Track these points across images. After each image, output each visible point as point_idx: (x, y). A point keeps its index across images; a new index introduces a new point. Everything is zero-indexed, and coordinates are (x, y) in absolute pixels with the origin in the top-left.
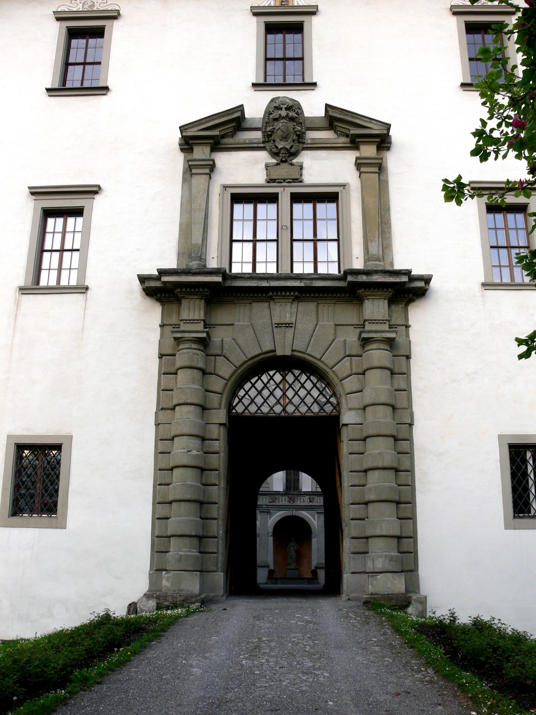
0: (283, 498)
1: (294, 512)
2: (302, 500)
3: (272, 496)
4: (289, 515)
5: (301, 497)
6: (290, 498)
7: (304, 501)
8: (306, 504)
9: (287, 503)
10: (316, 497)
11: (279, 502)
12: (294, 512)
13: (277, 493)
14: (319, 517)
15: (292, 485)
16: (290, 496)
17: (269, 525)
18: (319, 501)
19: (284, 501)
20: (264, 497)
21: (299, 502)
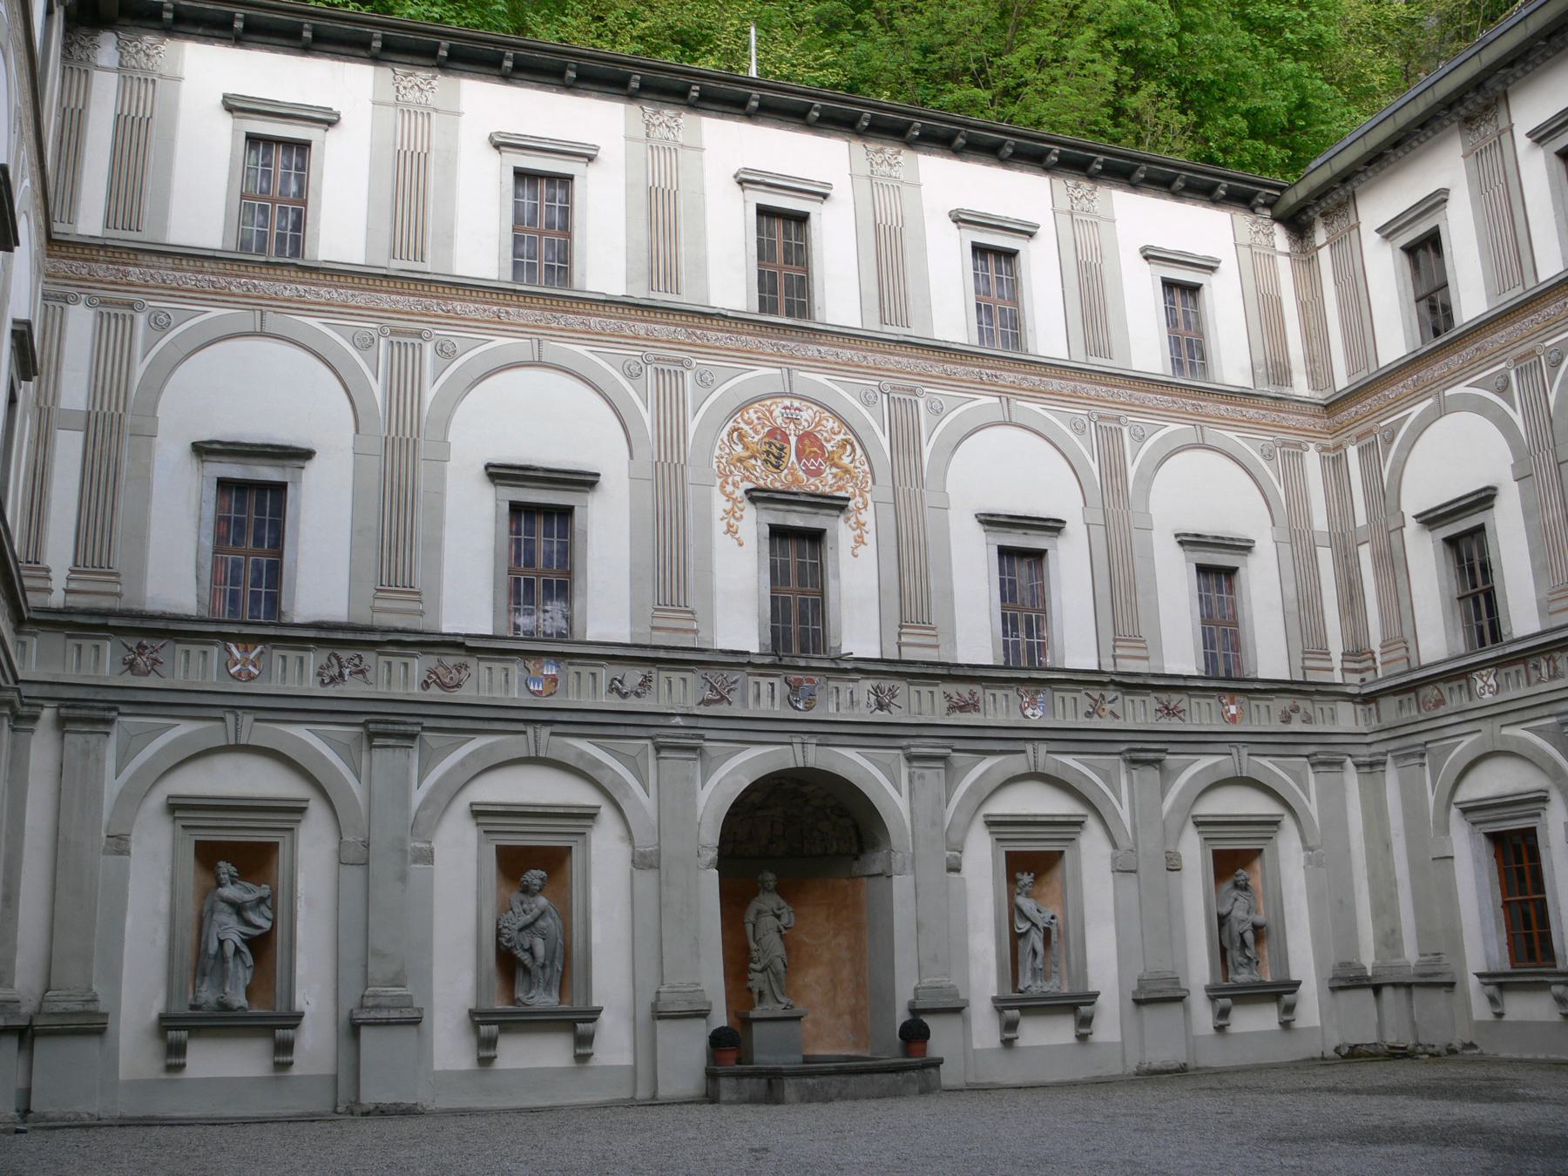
0: (765, 683)
1: (811, 749)
2: (845, 697)
3: (714, 674)
4: (792, 765)
5: (842, 686)
6: (795, 688)
7: (851, 702)
8: (864, 713)
9: (780, 710)
10: (901, 686)
11: (744, 700)
12: (811, 749)
13: (736, 661)
14: (922, 777)
15: (795, 627)
16: (793, 676)
17: (700, 811)
18: (915, 707)
19: (764, 697)
20: (676, 676)
21: (832, 708)
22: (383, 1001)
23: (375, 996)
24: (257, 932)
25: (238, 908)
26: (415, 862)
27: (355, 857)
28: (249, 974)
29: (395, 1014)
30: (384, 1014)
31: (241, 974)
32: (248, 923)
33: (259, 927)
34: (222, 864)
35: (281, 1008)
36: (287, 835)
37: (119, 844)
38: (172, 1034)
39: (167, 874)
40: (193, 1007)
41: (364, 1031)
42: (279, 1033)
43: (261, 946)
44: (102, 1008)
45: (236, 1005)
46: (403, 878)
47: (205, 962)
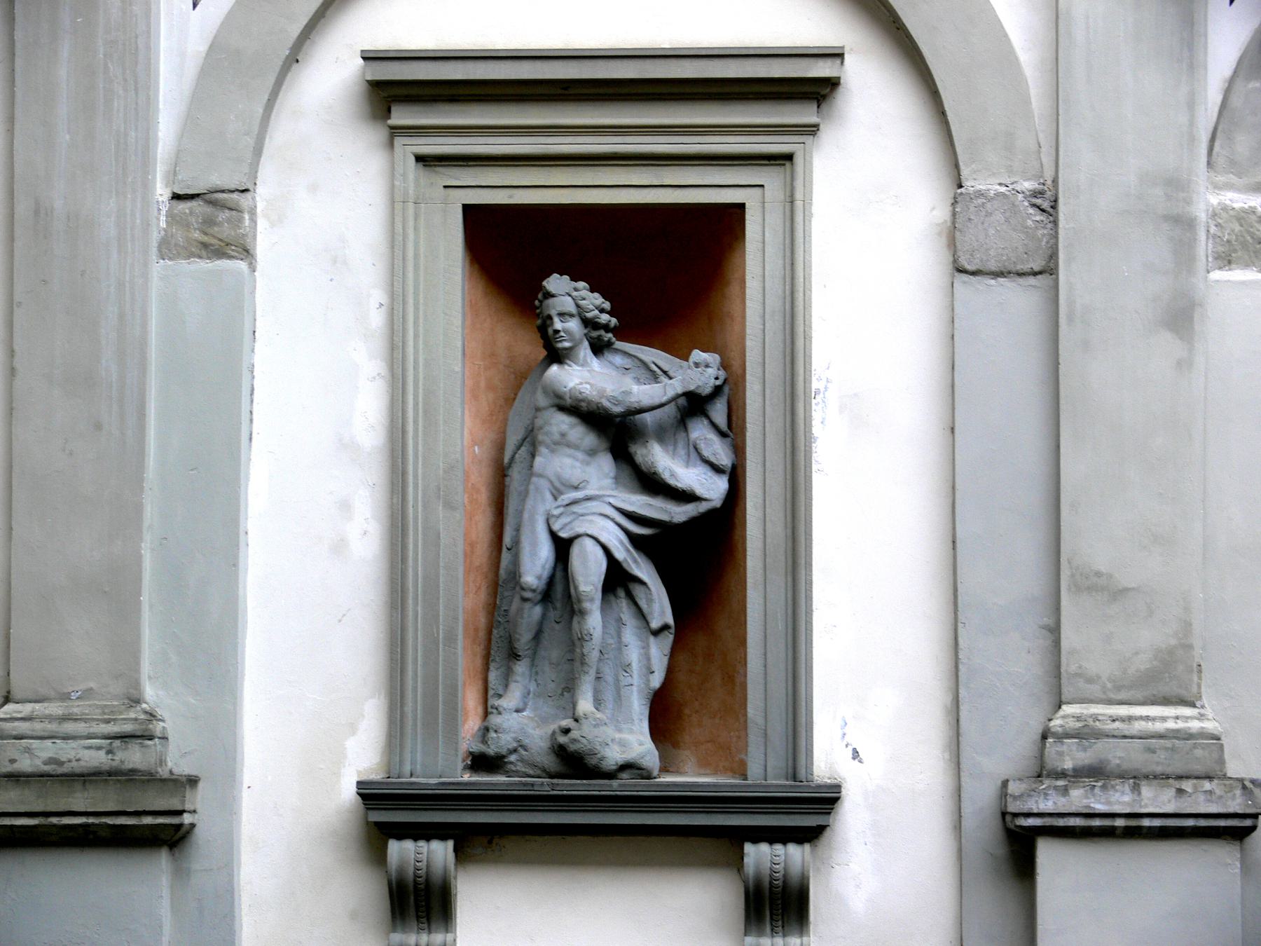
22: (1116, 754)
23: (1085, 734)
24: (679, 513)
25: (616, 431)
26: (1226, 260)
27: (1008, 247)
28: (659, 652)
29: (1157, 800)
30: (1120, 800)
31: (633, 655)
32: (652, 484)
33: (685, 496)
34: (557, 283)
35: (762, 769)
36: (770, 177)
37: (213, 221)
38: (401, 851)
39: (377, 319)
40: (481, 762)
41: (1048, 854)
42: (758, 855)
43: (698, 561)
44: (177, 762)
45: (613, 756)
46: (1181, 317)
47: (524, 619)
